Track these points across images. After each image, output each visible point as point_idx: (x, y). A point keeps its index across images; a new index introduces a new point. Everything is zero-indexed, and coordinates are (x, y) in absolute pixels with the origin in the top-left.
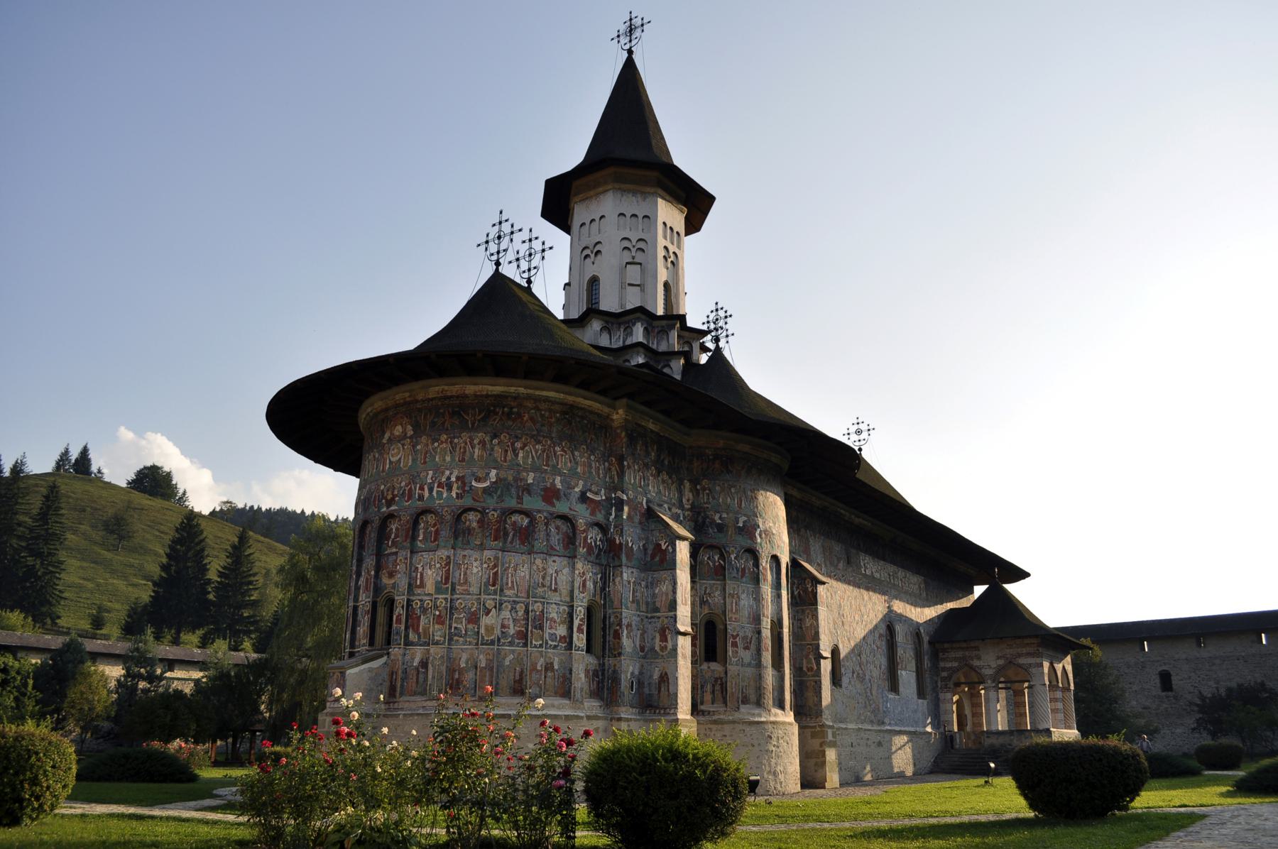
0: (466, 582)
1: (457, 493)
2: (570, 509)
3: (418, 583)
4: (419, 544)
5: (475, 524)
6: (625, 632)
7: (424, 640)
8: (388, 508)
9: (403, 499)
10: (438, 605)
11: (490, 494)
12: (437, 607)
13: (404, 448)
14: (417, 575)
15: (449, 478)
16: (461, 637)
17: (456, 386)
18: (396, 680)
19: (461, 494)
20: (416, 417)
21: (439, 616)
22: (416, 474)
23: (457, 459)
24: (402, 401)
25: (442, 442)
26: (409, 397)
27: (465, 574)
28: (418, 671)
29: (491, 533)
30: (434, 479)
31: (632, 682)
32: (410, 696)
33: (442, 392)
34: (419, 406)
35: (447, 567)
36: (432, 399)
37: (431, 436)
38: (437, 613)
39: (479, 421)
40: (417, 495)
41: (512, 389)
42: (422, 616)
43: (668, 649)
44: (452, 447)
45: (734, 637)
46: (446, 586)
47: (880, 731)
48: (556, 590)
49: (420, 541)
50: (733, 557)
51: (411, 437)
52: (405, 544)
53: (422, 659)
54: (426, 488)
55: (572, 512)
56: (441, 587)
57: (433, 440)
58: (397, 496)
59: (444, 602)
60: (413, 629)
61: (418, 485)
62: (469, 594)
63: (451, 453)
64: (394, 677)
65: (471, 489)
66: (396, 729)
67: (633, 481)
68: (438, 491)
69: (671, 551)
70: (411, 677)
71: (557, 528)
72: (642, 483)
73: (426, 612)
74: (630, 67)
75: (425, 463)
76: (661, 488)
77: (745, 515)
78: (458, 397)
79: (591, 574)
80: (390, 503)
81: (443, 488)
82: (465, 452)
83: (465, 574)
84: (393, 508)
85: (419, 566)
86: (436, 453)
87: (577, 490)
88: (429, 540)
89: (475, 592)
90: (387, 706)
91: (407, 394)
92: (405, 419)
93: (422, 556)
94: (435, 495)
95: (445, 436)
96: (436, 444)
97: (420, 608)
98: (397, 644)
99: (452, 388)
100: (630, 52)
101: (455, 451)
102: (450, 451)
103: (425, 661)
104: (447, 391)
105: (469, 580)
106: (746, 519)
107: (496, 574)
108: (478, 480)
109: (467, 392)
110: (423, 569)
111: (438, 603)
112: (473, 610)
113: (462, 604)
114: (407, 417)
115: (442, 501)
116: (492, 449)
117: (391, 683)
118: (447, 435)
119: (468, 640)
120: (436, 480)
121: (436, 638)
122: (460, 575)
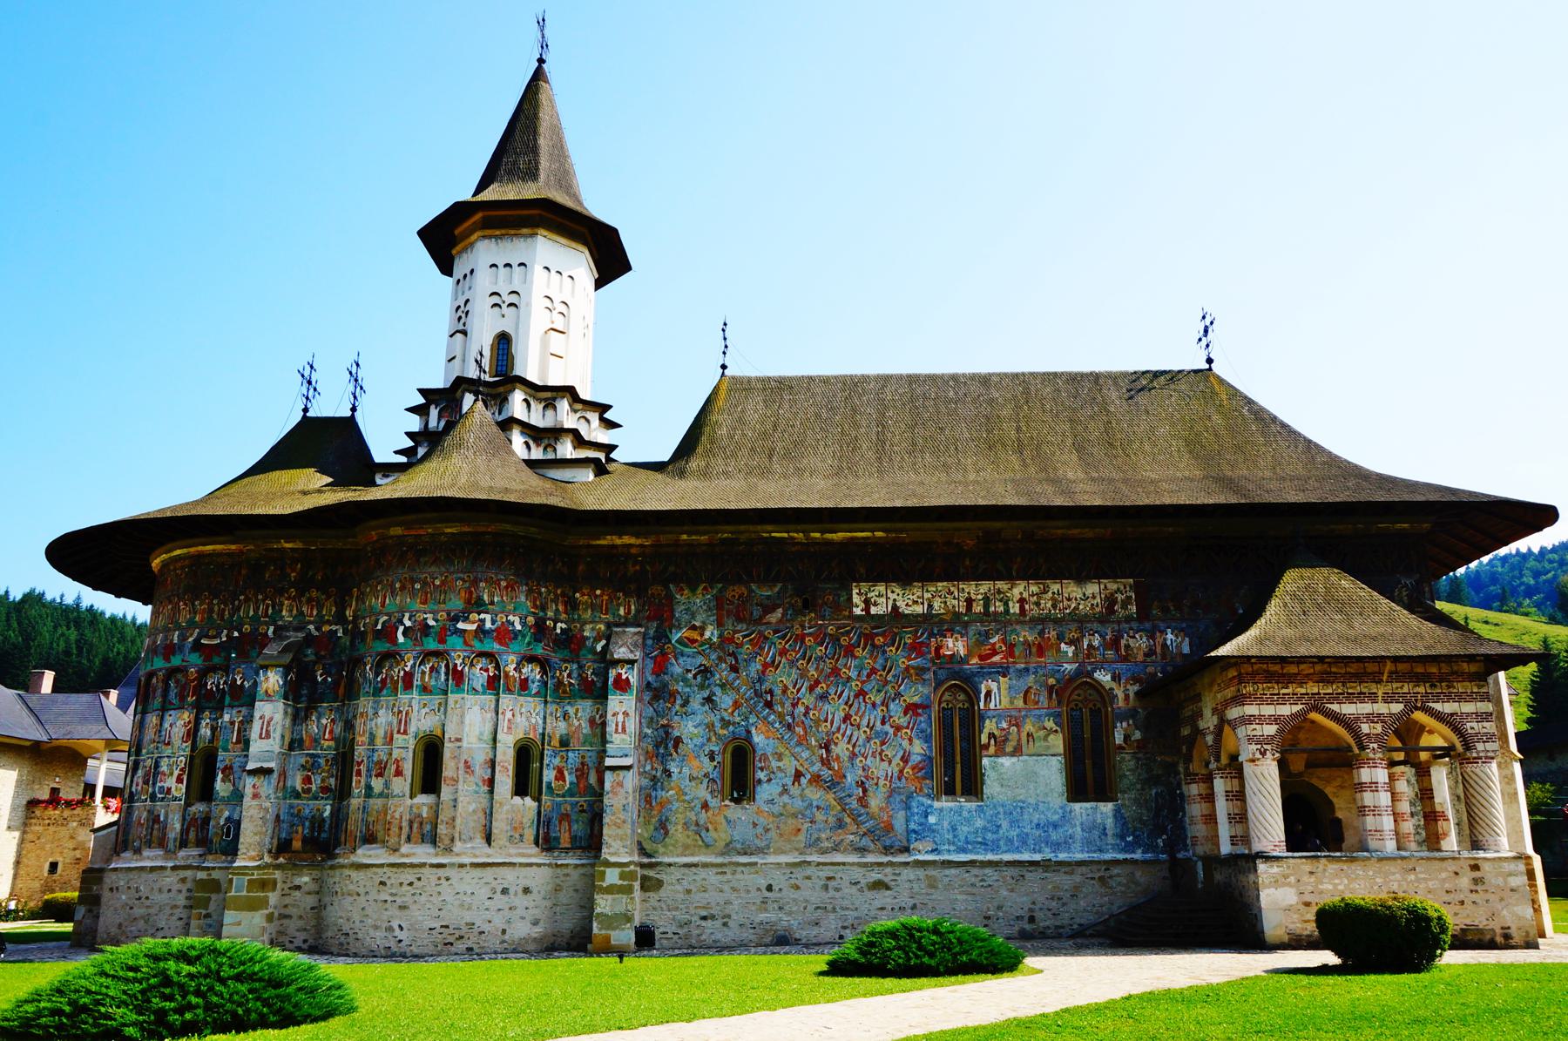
2: (183, 661)
6: (220, 776)
31: (229, 828)
45: (359, 764)
47: (891, 864)
48: (169, 744)
50: (368, 668)
55: (184, 664)
67: (251, 613)
71: (177, 682)
72: (270, 611)
74: (538, 76)
76: (304, 609)
77: (387, 614)
79: (208, 720)
87: (191, 639)
100: (541, 61)
106: (386, 618)
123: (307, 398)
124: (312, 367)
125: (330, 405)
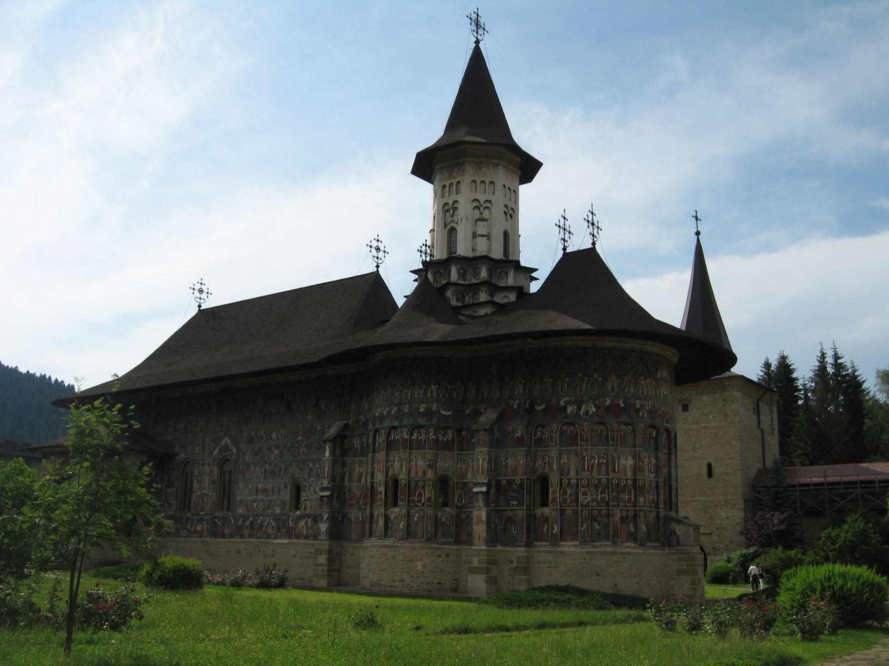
100: (477, 42)
123: (593, 235)
124: (592, 213)
125: (579, 242)
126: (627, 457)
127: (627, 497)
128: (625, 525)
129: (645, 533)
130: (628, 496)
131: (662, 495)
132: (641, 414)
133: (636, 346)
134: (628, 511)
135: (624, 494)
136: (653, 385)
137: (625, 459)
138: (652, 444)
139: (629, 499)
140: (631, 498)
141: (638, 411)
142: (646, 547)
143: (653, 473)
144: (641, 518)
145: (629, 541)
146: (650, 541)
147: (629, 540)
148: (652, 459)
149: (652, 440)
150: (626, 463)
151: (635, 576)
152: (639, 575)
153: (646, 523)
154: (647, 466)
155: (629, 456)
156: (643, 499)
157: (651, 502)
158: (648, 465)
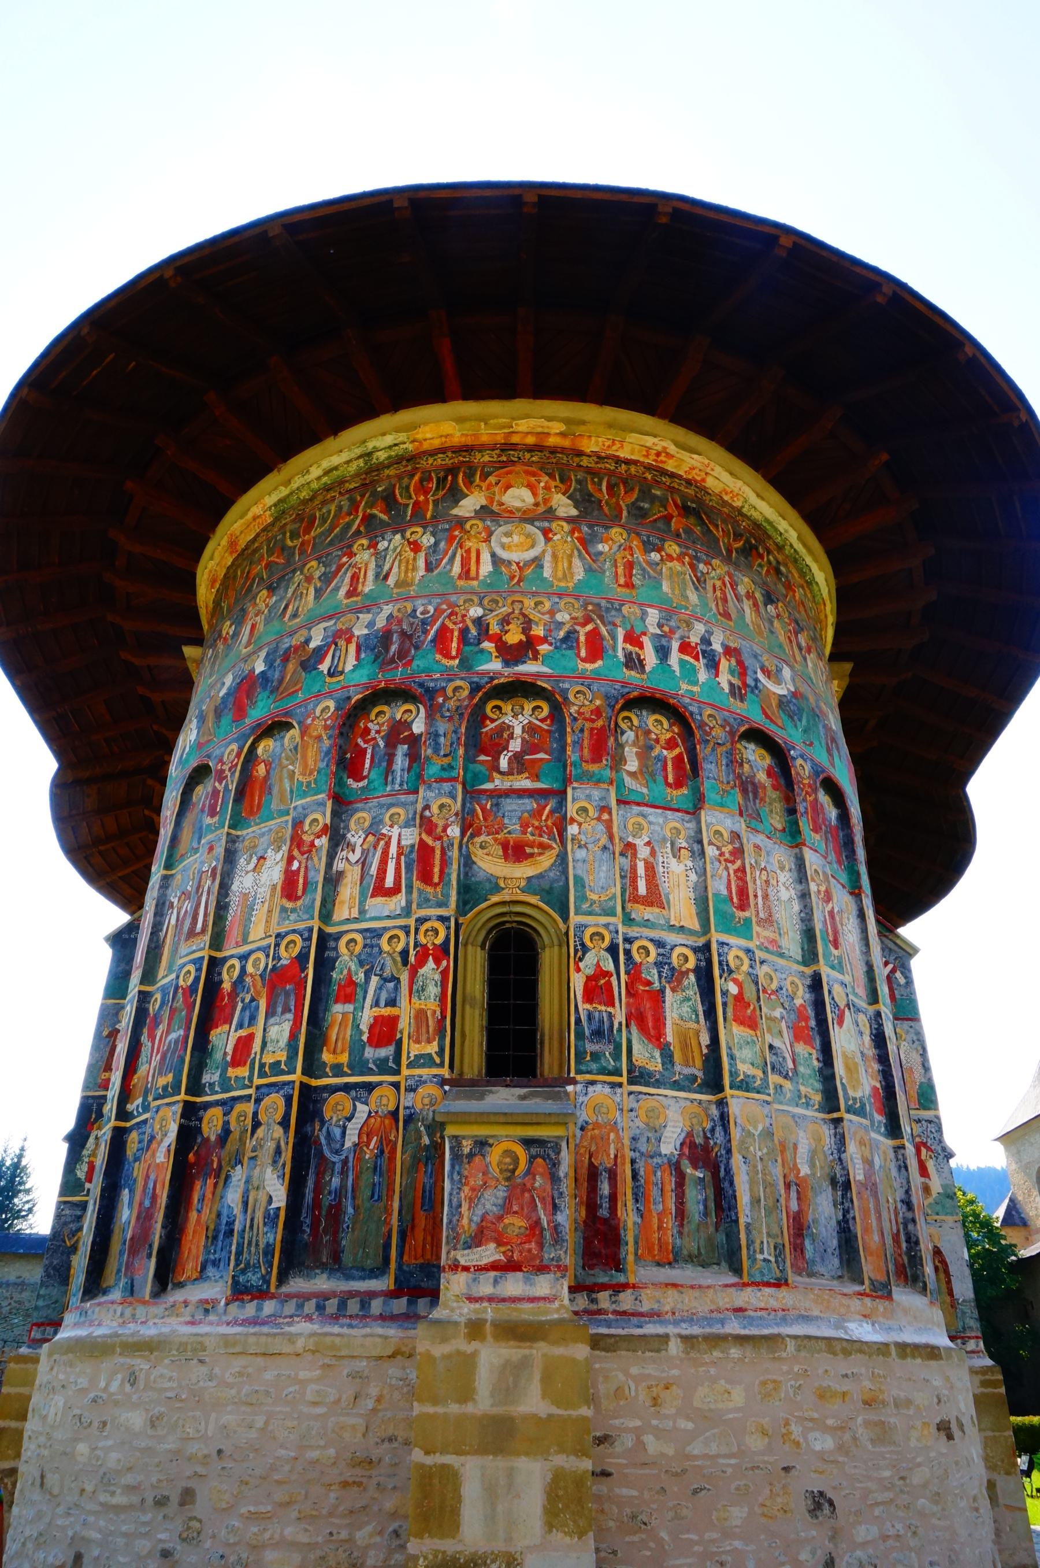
0: (769, 920)
1: (731, 685)
3: (642, 889)
4: (628, 781)
5: (762, 777)
7: (687, 1071)
8: (507, 663)
9: (569, 653)
10: (732, 965)
11: (791, 717)
12: (731, 972)
13: (548, 539)
14: (634, 869)
15: (706, 641)
16: (786, 1077)
17: (695, 456)
18: (613, 1198)
19: (739, 689)
20: (579, 482)
21: (739, 998)
22: (603, 603)
23: (714, 607)
24: (531, 440)
25: (670, 558)
26: (562, 434)
27: (766, 897)
28: (681, 1178)
29: (806, 808)
30: (666, 629)
32: (659, 1264)
33: (658, 454)
34: (585, 462)
35: (739, 863)
36: (628, 462)
37: (638, 534)
38: (734, 989)
39: (737, 552)
40: (620, 654)
41: (783, 525)
42: (668, 991)
43: (934, 1194)
44: (695, 576)
46: (742, 914)
49: (632, 774)
51: (569, 520)
52: (593, 768)
53: (690, 1134)
54: (646, 641)
56: (733, 916)
57: (644, 543)
58: (544, 640)
59: (747, 962)
60: (643, 1029)
61: (620, 633)
62: (781, 955)
63: (697, 589)
64: (605, 1188)
65: (756, 687)
66: (655, 1401)
68: (681, 661)
69: (902, 981)
70: (655, 1192)
73: (680, 982)
75: (629, 585)
78: (689, 482)
80: (512, 654)
81: (697, 658)
82: (725, 600)
83: (766, 897)
84: (529, 668)
85: (639, 842)
86: (661, 573)
88: (660, 779)
89: (791, 954)
90: (582, 1302)
91: (558, 427)
92: (547, 478)
93: (644, 816)
94: (676, 667)
95: (678, 549)
96: (655, 556)
97: (658, 965)
98: (604, 1071)
99: (685, 455)
101: (705, 589)
102: (693, 583)
103: (699, 1140)
104: (670, 456)
105: (776, 916)
107: (831, 913)
108: (767, 673)
109: (710, 482)
110: (653, 853)
111: (731, 958)
112: (798, 1002)
113: (772, 979)
114: (552, 476)
115: (695, 689)
116: (771, 623)
117: (592, 1206)
118: (679, 545)
119: (802, 1088)
120: (672, 631)
121: (744, 1068)
122: (756, 896)
126: (262, 858)
127: (234, 1037)
128: (210, 1182)
129: (271, 1219)
130: (242, 1033)
131: (433, 990)
132: (324, 667)
133: (336, 460)
134: (228, 1105)
135: (226, 1027)
136: (416, 547)
137: (254, 870)
138: (400, 761)
139: (244, 1045)
140: (251, 1037)
141: (310, 661)
142: (269, 1307)
143: (395, 890)
144: (260, 1132)
145: (211, 1271)
146: (335, 1265)
147: (216, 1263)
148: (395, 831)
149: (402, 749)
150: (256, 883)
151: (161, 1502)
152: (188, 1496)
153: (287, 1155)
154: (358, 869)
155: (270, 853)
156: (287, 1027)
157: (365, 1038)
158: (364, 863)
